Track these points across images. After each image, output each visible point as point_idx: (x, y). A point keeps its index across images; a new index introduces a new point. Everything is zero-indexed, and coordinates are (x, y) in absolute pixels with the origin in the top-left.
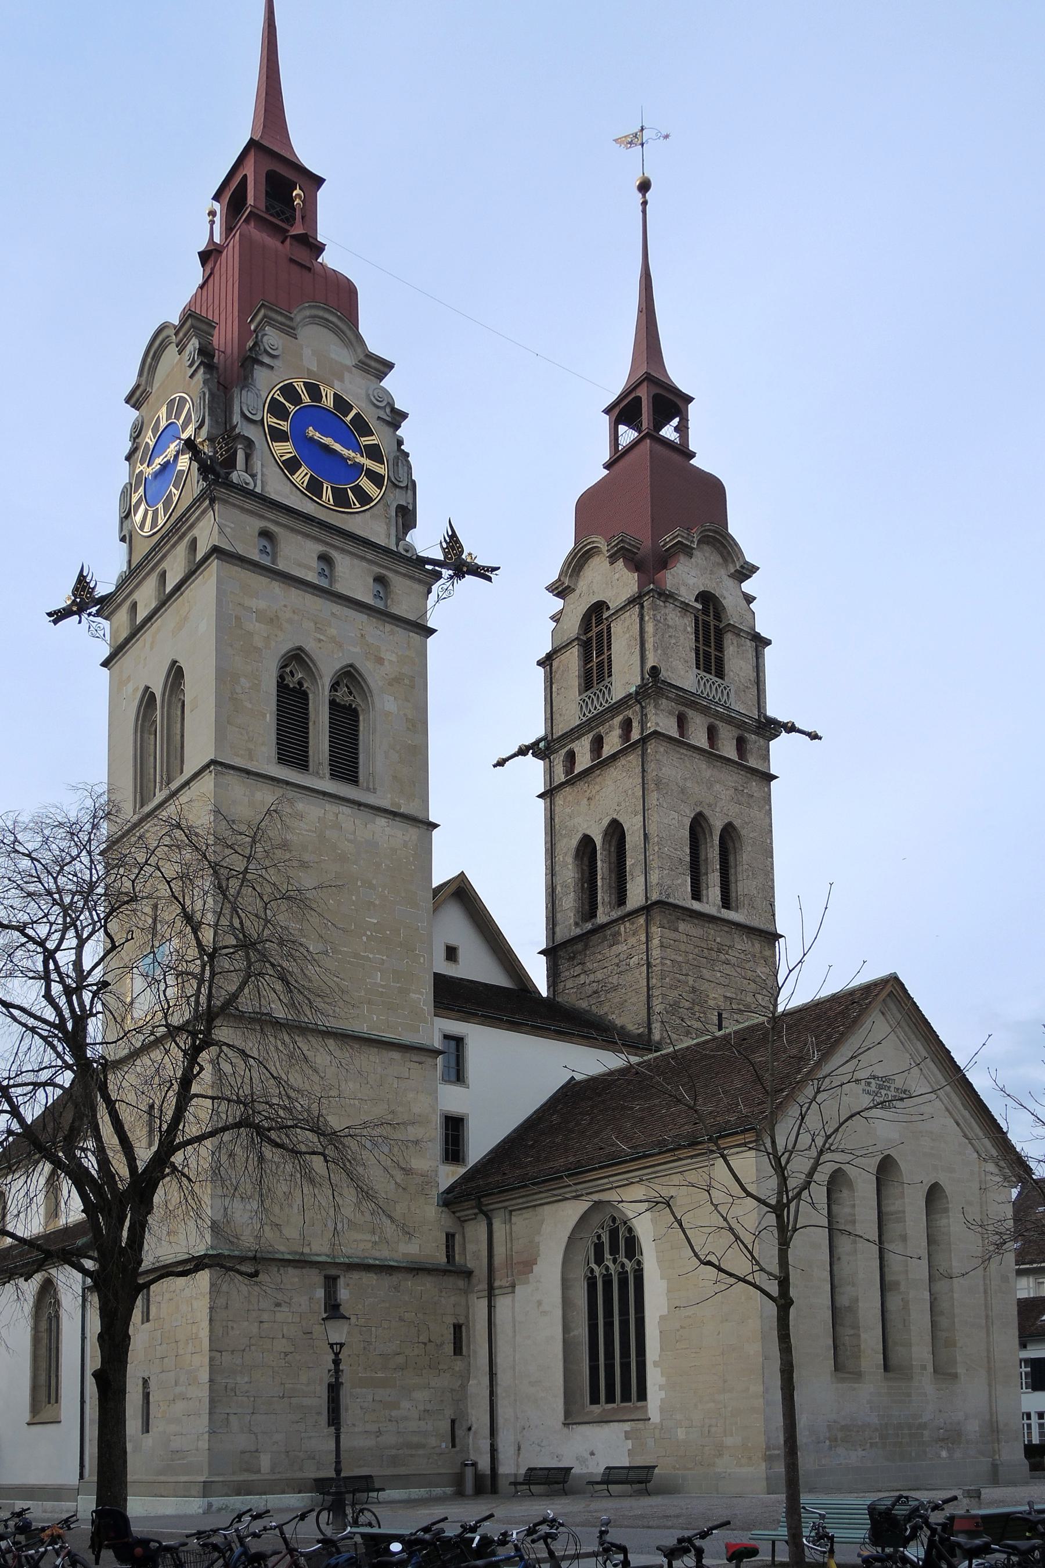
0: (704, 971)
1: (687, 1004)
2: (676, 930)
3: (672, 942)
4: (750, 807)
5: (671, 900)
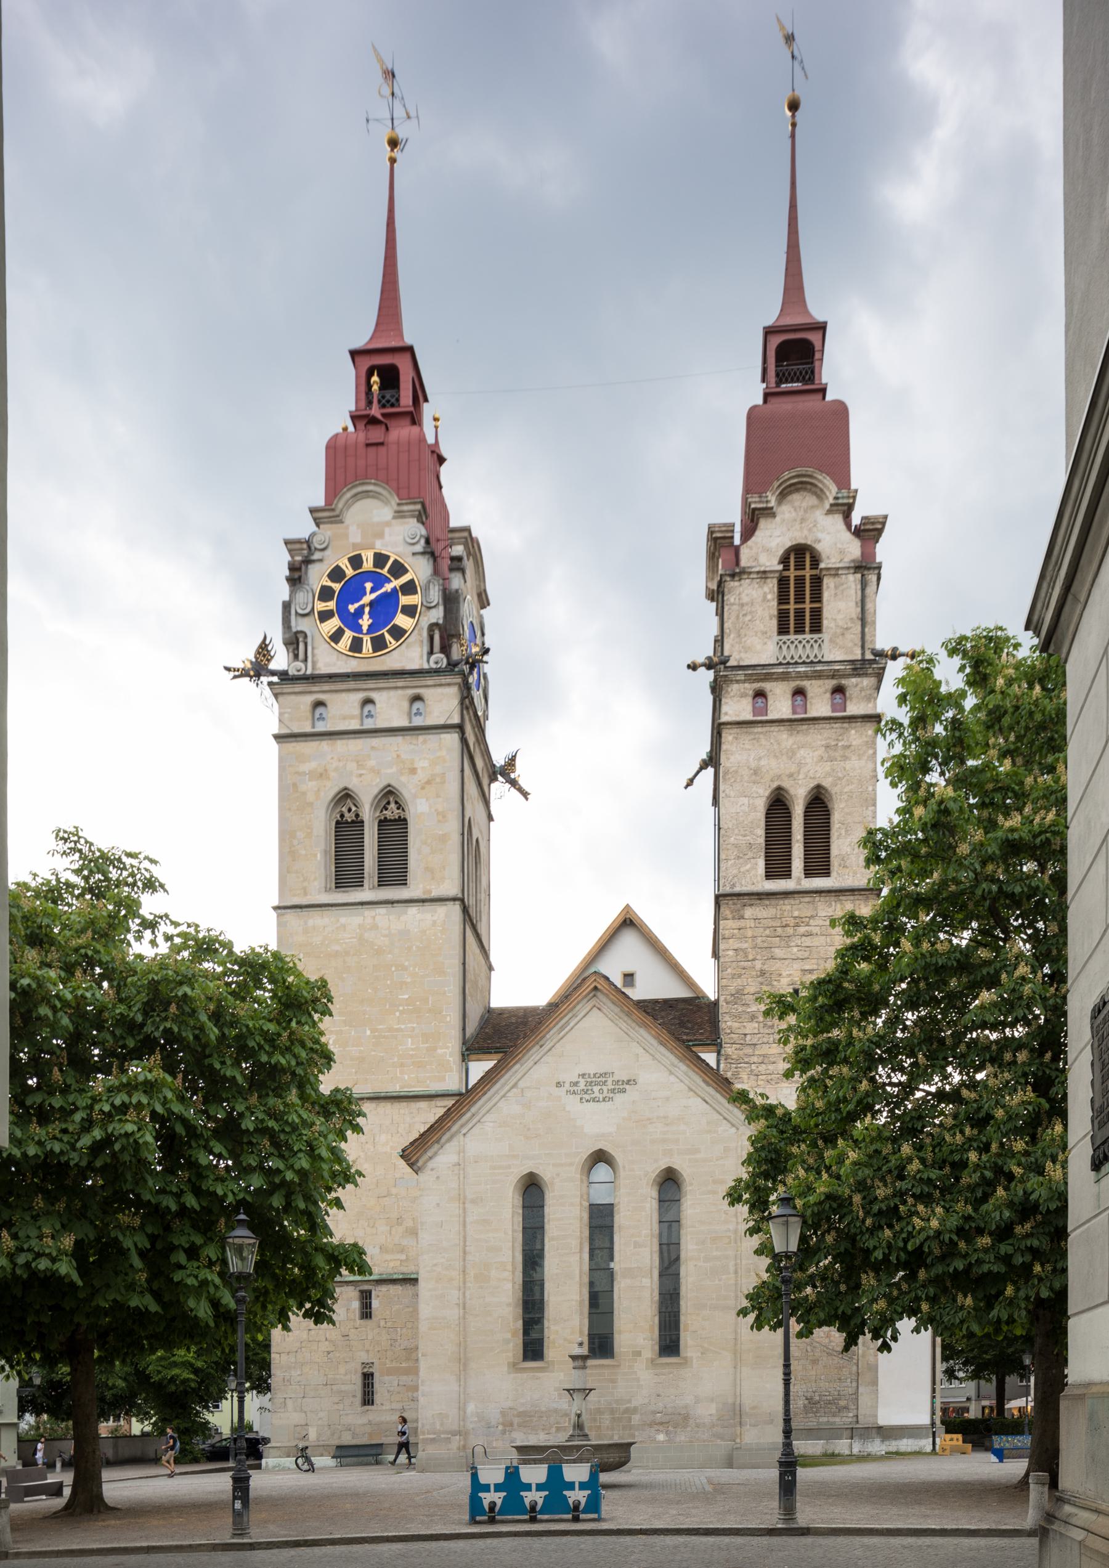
0: (777, 951)
1: (752, 990)
2: (742, 917)
3: (736, 931)
4: (845, 758)
5: (737, 889)
